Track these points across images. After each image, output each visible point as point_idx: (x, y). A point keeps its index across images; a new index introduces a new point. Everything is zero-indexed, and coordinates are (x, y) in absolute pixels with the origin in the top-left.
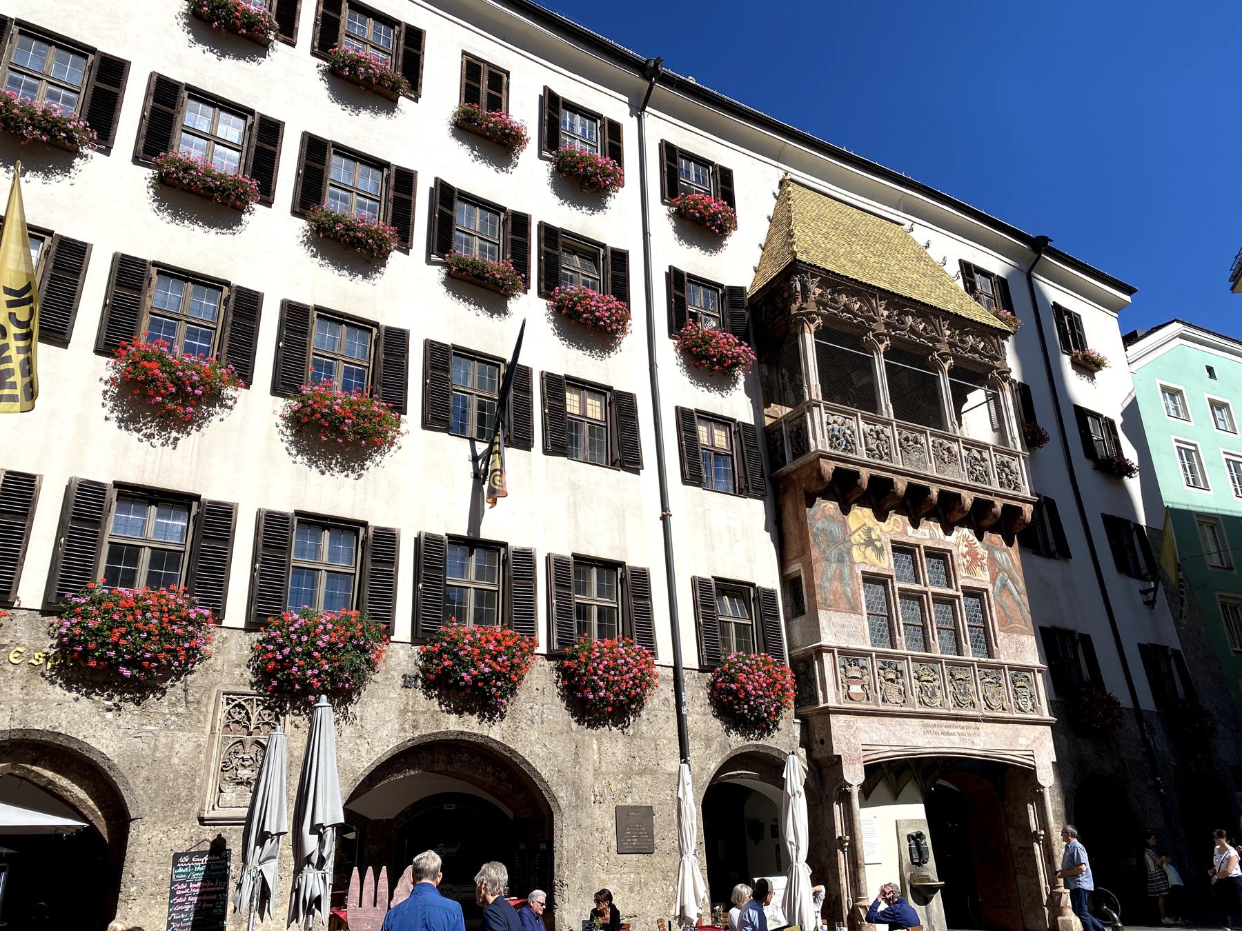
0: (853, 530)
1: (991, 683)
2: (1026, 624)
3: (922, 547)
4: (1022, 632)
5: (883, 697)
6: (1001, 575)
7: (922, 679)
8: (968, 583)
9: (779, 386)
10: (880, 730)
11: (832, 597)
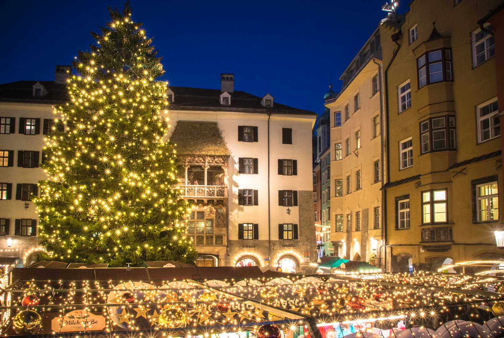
2: (224, 225)
4: (223, 227)
8: (208, 218)
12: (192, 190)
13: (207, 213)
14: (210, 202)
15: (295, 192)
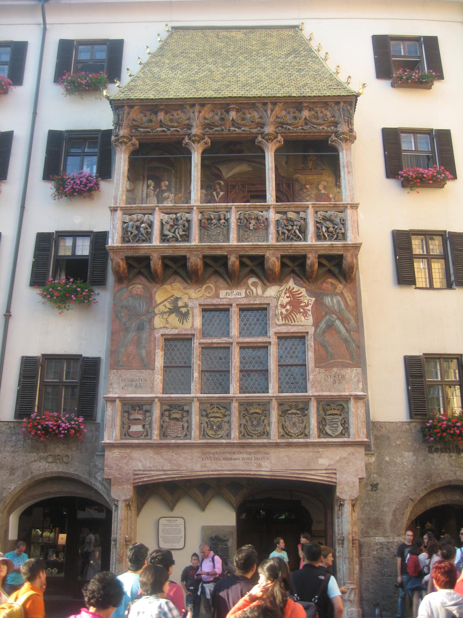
0: (158, 302)
1: (295, 414)
2: (352, 358)
3: (234, 305)
5: (164, 433)
6: (328, 317)
7: (210, 415)
8: (284, 329)
9: (142, 195)
10: (154, 458)
11: (125, 359)
12: (220, 219)
13: (280, 310)
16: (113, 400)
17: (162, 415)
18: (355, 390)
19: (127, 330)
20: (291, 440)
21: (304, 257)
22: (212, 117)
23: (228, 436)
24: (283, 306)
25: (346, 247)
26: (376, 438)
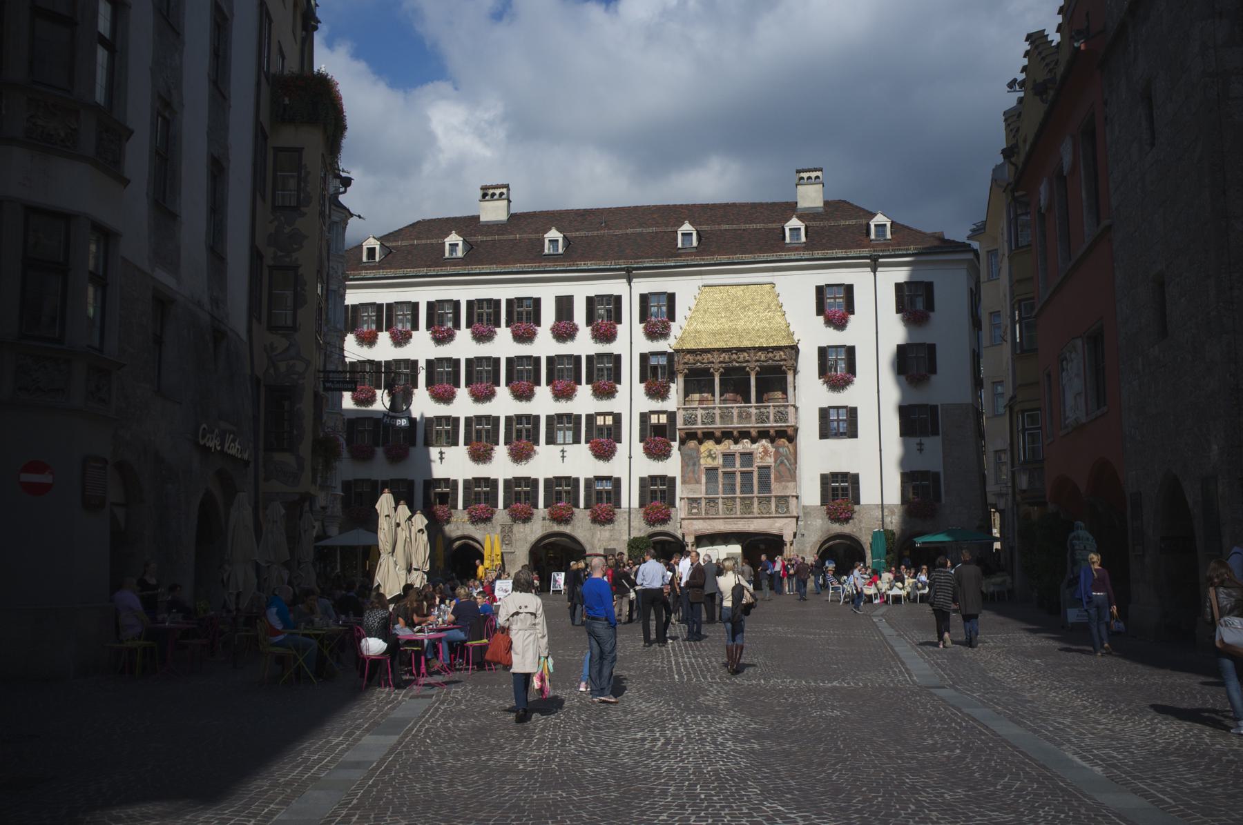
4: (789, 481)
14: (763, 434)
15: (934, 409)
16: (684, 499)
17: (706, 505)
18: (793, 492)
19: (688, 466)
20: (763, 515)
21: (769, 432)
22: (724, 357)
23: (736, 513)
24: (760, 453)
25: (787, 426)
26: (805, 513)
